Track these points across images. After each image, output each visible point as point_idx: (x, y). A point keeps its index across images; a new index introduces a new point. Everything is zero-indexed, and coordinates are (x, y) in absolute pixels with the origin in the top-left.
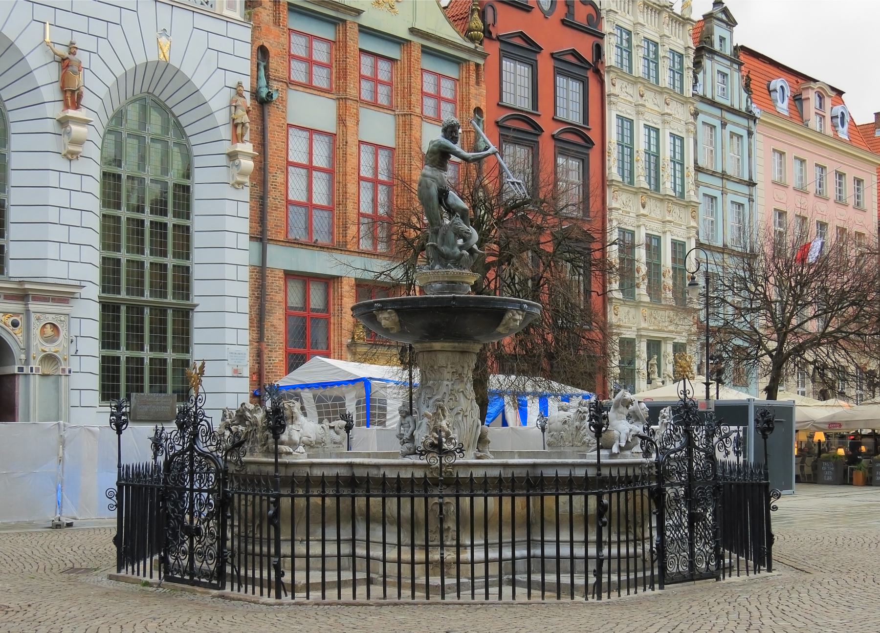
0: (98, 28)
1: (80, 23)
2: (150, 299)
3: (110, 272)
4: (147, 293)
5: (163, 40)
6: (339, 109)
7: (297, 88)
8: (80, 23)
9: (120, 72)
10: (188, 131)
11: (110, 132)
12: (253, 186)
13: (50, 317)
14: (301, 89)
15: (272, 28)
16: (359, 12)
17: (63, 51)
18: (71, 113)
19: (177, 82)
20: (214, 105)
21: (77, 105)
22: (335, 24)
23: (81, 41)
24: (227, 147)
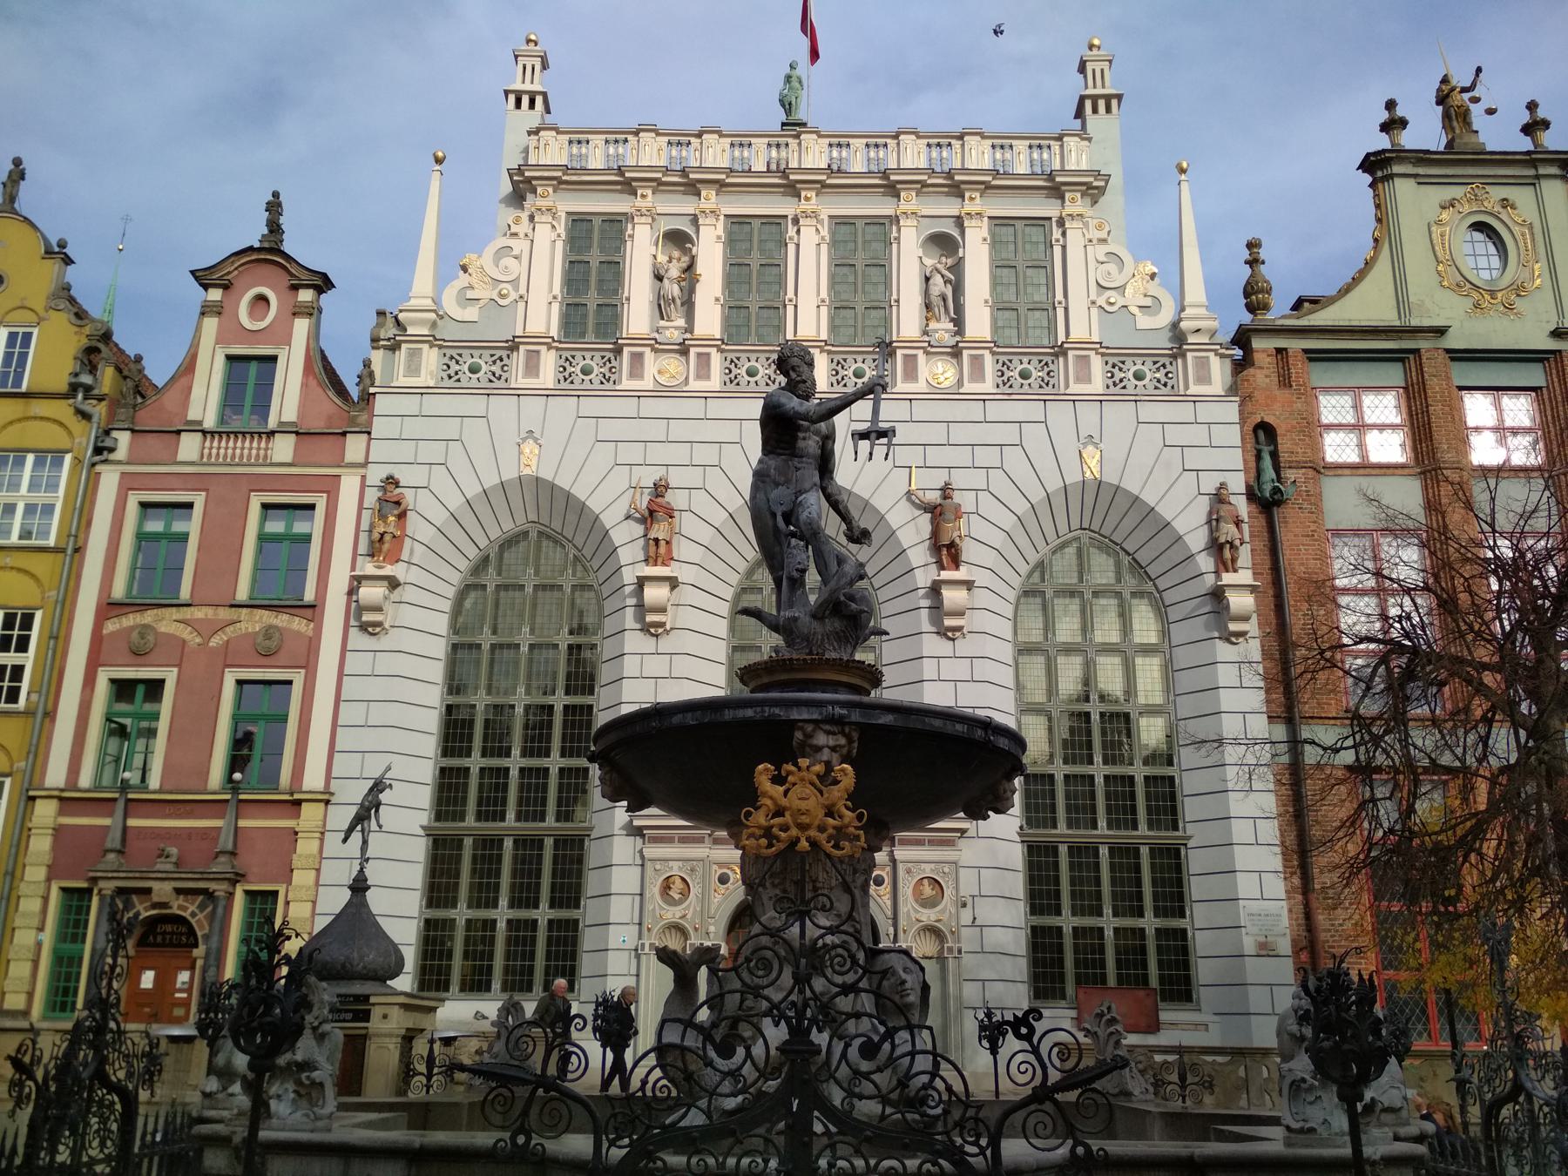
0: (987, 457)
1: (962, 456)
4: (1102, 823)
5: (1089, 450)
6: (1425, 488)
7: (1340, 472)
8: (962, 456)
9: (1021, 507)
10: (1153, 571)
11: (1026, 593)
12: (1265, 637)
13: (928, 867)
14: (1347, 472)
15: (1277, 393)
16: (1440, 331)
17: (934, 497)
18: (945, 575)
19: (1121, 504)
20: (1180, 526)
21: (956, 562)
22: (1402, 360)
23: (959, 479)
24: (1210, 580)
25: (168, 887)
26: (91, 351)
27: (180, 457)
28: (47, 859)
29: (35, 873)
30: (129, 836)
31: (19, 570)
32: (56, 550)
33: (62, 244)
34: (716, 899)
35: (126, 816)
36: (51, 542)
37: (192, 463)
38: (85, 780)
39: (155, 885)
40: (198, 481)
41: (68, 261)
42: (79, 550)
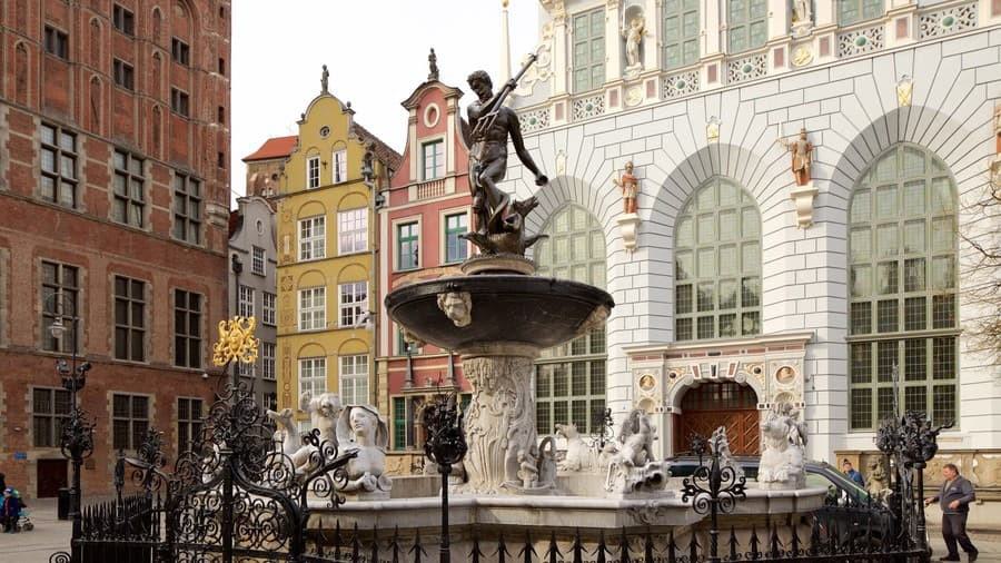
2: (905, 332)
3: (858, 314)
25: (431, 394)
26: (368, 155)
27: (410, 200)
28: (386, 386)
29: (383, 393)
30: (417, 374)
31: (359, 264)
32: (370, 253)
33: (349, 105)
34: (670, 386)
35: (412, 366)
36: (367, 249)
37: (414, 202)
38: (395, 352)
39: (426, 394)
40: (419, 210)
41: (353, 113)
42: (377, 251)
